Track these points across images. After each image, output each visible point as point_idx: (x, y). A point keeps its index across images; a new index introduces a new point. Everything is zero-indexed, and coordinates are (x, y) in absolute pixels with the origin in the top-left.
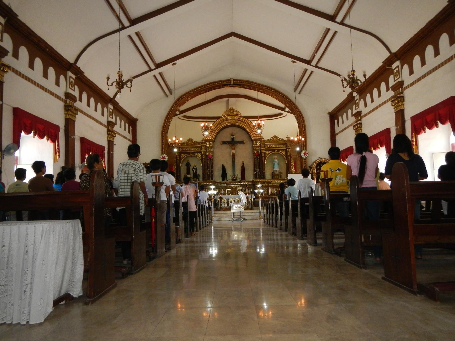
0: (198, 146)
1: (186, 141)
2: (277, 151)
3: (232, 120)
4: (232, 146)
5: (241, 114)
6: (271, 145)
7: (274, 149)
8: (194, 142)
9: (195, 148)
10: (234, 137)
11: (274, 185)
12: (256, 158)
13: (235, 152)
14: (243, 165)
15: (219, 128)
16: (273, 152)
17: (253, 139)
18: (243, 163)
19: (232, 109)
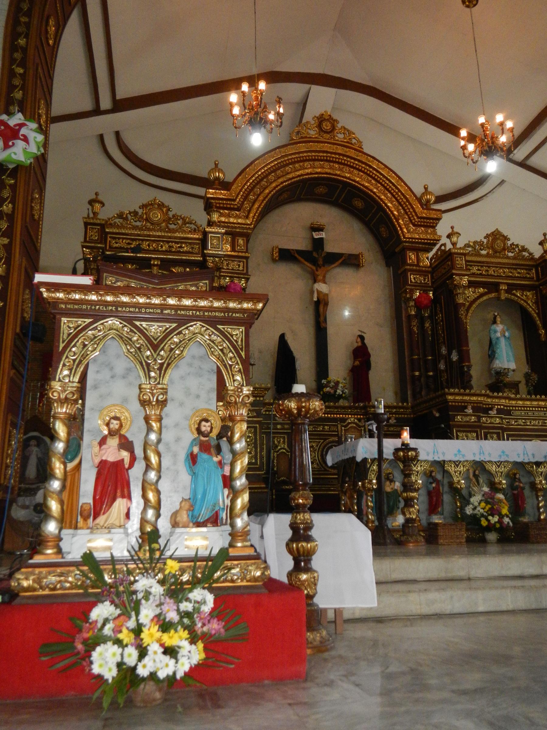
0: (190, 236)
1: (138, 210)
2: (507, 291)
3: (327, 161)
4: (318, 266)
5: (361, 142)
6: (482, 266)
7: (497, 285)
8: (171, 216)
9: (177, 243)
10: (323, 235)
11: (520, 422)
12: (416, 316)
13: (330, 291)
14: (360, 344)
15: (274, 185)
16: (493, 295)
17: (406, 242)
18: (362, 338)
19: (328, 120)
